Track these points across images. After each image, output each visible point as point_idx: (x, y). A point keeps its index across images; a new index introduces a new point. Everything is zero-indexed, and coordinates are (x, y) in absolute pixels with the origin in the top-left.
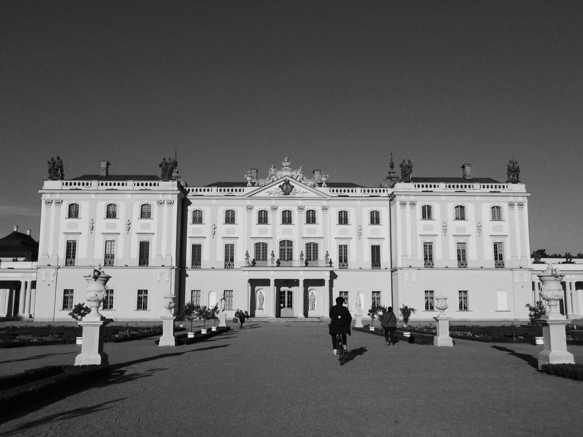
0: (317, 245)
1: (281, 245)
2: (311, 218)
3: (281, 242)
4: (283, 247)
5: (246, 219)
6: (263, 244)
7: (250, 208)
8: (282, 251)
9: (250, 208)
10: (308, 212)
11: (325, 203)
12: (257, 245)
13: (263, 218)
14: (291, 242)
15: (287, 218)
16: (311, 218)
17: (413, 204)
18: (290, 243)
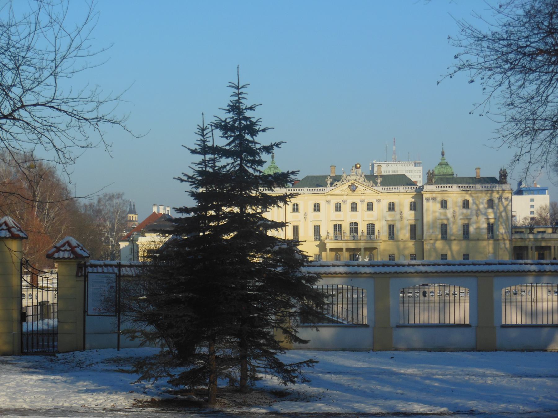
0: (374, 225)
1: (350, 225)
2: (370, 207)
3: (350, 223)
4: (351, 227)
5: (327, 210)
6: (339, 225)
7: (328, 202)
8: (351, 231)
9: (328, 202)
10: (368, 203)
11: (379, 197)
12: (335, 226)
13: (338, 208)
14: (357, 223)
15: (354, 207)
16: (370, 207)
17: (434, 199)
18: (356, 224)
